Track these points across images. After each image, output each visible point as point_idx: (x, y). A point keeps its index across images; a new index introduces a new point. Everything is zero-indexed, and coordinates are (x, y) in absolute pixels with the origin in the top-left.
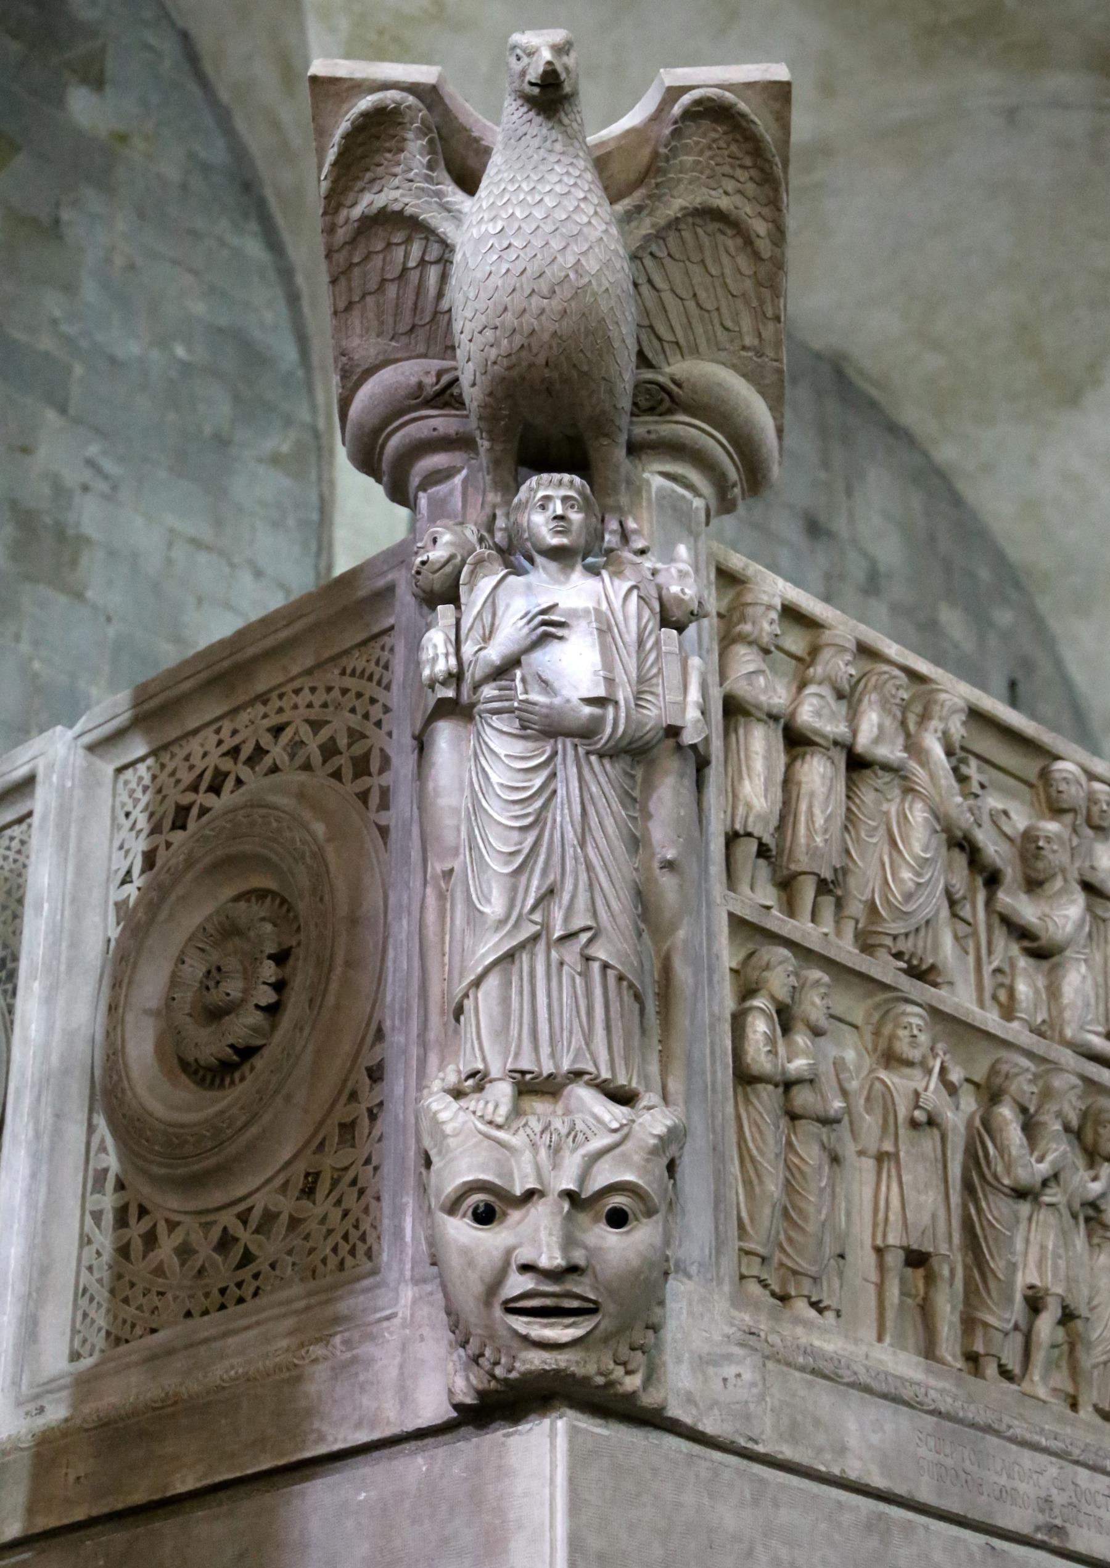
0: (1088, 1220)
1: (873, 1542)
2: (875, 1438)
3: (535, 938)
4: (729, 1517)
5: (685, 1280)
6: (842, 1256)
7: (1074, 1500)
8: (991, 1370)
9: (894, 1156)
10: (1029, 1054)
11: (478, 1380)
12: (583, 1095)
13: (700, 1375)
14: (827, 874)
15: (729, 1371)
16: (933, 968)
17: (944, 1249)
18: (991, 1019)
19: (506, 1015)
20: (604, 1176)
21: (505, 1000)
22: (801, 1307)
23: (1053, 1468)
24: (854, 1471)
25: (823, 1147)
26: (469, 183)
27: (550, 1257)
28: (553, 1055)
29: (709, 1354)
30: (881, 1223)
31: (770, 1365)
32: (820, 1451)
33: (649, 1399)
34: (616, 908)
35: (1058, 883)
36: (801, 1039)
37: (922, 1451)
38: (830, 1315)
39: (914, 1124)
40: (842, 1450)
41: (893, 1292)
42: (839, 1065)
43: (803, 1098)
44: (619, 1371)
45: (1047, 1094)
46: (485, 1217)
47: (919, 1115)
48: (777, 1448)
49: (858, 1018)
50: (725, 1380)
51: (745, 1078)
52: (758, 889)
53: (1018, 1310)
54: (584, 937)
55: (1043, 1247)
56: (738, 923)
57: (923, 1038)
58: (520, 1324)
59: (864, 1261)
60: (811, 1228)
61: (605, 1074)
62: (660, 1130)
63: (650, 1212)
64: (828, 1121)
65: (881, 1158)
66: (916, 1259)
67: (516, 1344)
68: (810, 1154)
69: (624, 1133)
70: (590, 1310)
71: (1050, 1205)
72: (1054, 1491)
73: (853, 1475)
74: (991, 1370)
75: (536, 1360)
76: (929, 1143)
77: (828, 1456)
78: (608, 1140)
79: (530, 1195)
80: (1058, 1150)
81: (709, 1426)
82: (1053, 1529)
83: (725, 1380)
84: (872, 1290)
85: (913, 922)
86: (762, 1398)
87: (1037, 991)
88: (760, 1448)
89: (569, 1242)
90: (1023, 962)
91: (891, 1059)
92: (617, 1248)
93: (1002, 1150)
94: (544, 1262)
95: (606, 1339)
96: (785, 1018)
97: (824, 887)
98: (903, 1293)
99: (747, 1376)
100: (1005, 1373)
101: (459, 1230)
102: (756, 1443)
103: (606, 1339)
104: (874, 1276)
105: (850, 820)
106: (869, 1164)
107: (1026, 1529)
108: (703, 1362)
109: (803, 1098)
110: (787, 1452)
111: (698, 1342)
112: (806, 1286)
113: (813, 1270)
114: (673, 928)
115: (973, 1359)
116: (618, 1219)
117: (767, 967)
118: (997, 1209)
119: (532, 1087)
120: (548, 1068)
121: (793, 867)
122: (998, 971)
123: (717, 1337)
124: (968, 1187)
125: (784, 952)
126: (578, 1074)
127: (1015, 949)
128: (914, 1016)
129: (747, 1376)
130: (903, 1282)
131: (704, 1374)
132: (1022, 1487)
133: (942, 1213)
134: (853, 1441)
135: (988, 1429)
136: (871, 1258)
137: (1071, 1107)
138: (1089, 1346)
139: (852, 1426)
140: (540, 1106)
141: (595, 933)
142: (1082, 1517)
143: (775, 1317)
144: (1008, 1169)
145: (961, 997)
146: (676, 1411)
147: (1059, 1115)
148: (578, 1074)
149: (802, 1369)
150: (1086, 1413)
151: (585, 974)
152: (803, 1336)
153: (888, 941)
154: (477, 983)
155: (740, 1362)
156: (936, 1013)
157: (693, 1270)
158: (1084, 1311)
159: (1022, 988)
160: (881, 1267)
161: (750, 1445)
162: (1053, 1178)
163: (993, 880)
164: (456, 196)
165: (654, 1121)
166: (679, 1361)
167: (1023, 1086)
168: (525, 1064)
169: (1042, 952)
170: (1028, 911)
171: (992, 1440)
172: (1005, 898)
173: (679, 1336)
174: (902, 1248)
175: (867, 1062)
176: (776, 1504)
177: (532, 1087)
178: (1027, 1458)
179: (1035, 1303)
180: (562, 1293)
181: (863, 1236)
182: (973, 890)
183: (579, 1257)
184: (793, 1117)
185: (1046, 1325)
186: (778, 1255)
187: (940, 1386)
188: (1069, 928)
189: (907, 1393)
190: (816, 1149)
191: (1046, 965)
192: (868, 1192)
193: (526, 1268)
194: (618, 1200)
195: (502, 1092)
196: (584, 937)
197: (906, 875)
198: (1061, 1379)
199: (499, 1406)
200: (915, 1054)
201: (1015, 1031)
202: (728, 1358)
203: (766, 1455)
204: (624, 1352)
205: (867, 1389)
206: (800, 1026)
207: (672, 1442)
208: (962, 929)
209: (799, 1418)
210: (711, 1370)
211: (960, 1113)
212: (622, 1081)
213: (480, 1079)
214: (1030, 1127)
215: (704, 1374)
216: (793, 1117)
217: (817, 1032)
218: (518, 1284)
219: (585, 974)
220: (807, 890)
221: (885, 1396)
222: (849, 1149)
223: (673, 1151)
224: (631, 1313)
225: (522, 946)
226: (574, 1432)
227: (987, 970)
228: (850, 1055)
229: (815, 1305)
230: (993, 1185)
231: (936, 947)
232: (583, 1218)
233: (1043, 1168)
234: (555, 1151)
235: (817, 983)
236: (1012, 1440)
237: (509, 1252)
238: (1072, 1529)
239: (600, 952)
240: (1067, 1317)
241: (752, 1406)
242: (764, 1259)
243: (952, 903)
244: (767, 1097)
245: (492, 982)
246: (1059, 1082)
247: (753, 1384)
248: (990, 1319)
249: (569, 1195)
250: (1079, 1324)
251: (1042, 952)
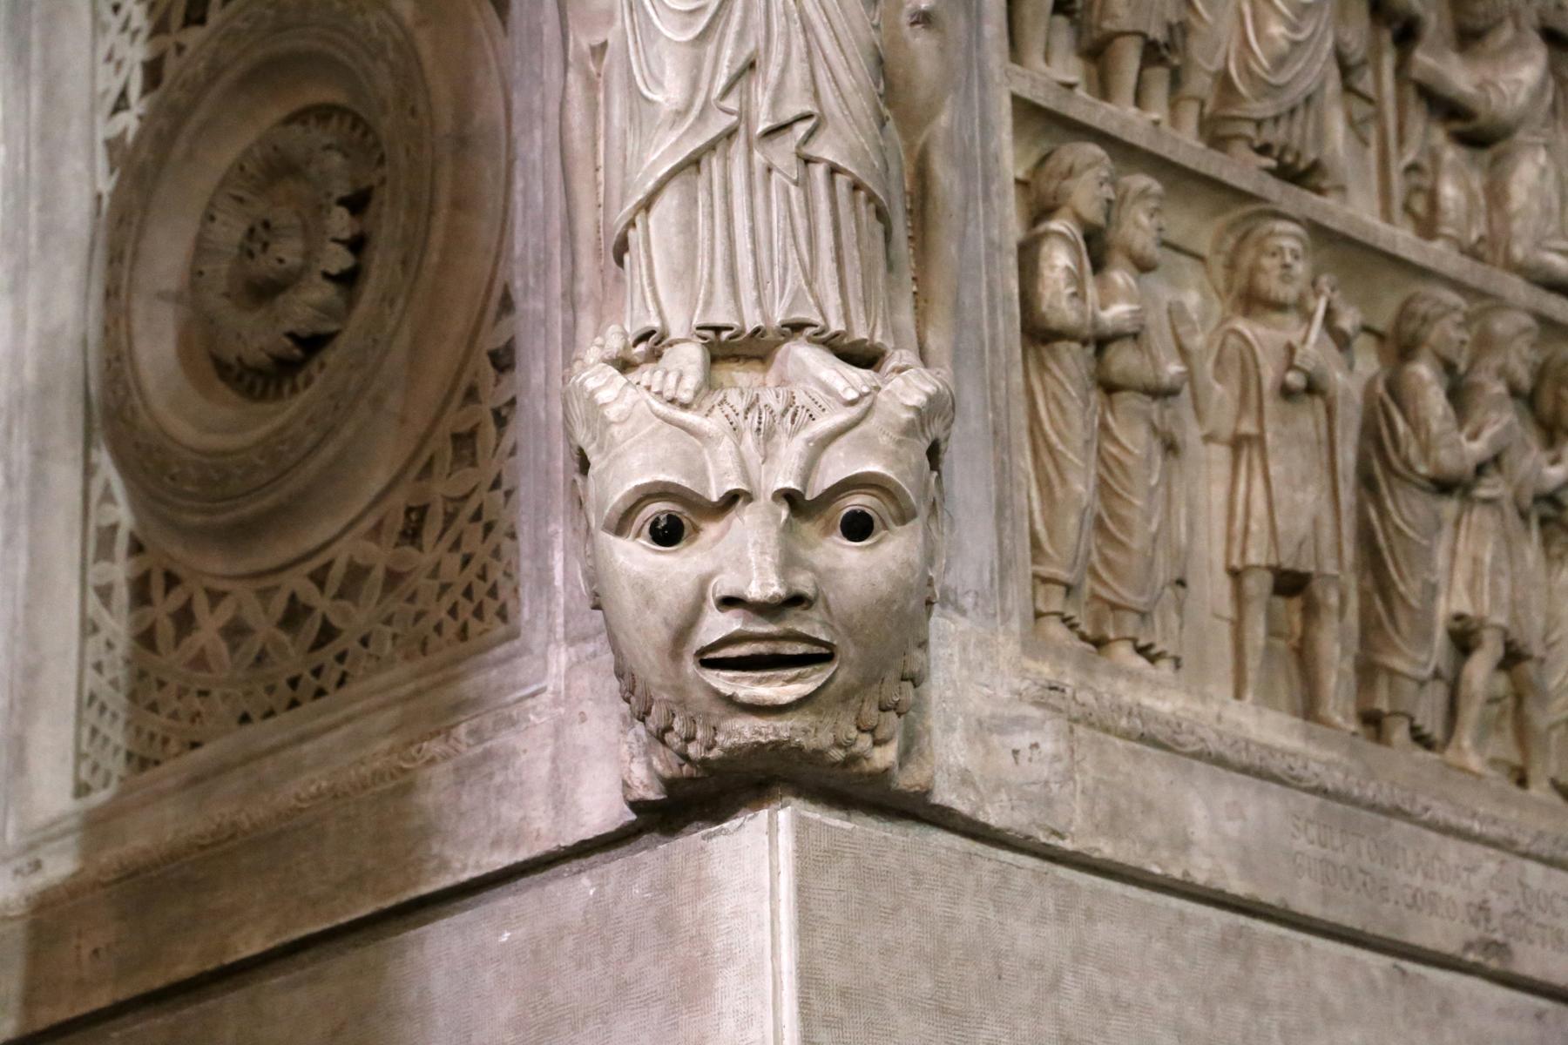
0: (1544, 521)
1: (1231, 966)
2: (1232, 828)
3: (730, 134)
4: (1025, 936)
5: (956, 616)
6: (1181, 583)
7: (1522, 907)
8: (1400, 734)
9: (1260, 440)
10: (1457, 285)
11: (666, 763)
12: (804, 356)
13: (979, 747)
14: (1157, 33)
15: (1022, 740)
16: (1315, 167)
17: (1330, 568)
18: (1402, 239)
19: (691, 247)
20: (837, 467)
21: (689, 228)
22: (1123, 652)
23: (1490, 863)
24: (1201, 871)
25: (1154, 430)
27: (763, 585)
28: (759, 302)
29: (993, 716)
30: (1236, 536)
31: (1080, 730)
32: (1152, 845)
33: (908, 780)
34: (847, 88)
35: (1507, 33)
36: (1120, 276)
37: (1301, 844)
38: (1165, 666)
39: (1286, 392)
40: (1184, 844)
41: (1257, 631)
42: (1176, 313)
43: (1123, 360)
44: (865, 741)
45: (1485, 343)
46: (668, 534)
47: (1295, 379)
48: (1092, 844)
49: (1204, 245)
50: (1015, 752)
51: (1039, 334)
52: (1057, 59)
54: (801, 129)
55: (1476, 561)
56: (1026, 110)
57: (1300, 268)
58: (722, 681)
59: (1213, 589)
60: (1136, 544)
61: (836, 325)
62: (917, 399)
63: (904, 517)
64: (1161, 393)
65: (1238, 443)
66: (1290, 583)
67: (717, 710)
68: (1134, 439)
69: (865, 407)
70: (822, 656)
71: (1488, 501)
72: (1492, 895)
73: (1200, 878)
74: (1400, 734)
75: (746, 730)
76: (1308, 418)
77: (1165, 854)
78: (843, 416)
79: (732, 499)
80: (1499, 421)
81: (994, 816)
82: (1489, 946)
83: (1015, 752)
84: (1225, 630)
85: (1287, 99)
86: (1068, 777)
87: (1471, 196)
88: (1068, 845)
89: (789, 563)
90: (1451, 153)
91: (1253, 301)
92: (857, 569)
93: (1416, 425)
94: (754, 592)
95: (846, 696)
96: (1097, 247)
97: (1153, 53)
98: (1273, 632)
99: (1048, 747)
100: (1420, 739)
101: (633, 556)
102: (1061, 836)
103: (846, 696)
104: (1228, 610)
106: (1220, 453)
107: (1451, 947)
108: (983, 729)
109: (1123, 360)
110: (1106, 849)
111: (977, 701)
112: (1130, 623)
113: (1139, 601)
114: (932, 110)
115: (1373, 722)
116: (858, 528)
117: (1070, 173)
118: (1409, 510)
119: (731, 349)
120: (752, 320)
121: (1108, 25)
122: (1413, 168)
123: (1003, 694)
124: (1367, 481)
125: (1094, 150)
126: (796, 328)
127: (1439, 135)
128: (1287, 237)
129: (1048, 747)
130: (1271, 617)
131: (985, 743)
132: (1445, 890)
133: (1327, 519)
134: (1200, 832)
135: (1396, 812)
136: (1224, 585)
137: (1520, 360)
138: (1544, 698)
139: (1198, 812)
140: (741, 377)
141: (816, 122)
142: (1533, 929)
143: (1085, 666)
144: (1426, 450)
145: (1358, 209)
146: (946, 795)
147: (1502, 373)
148: (797, 328)
149: (1126, 735)
150: (1539, 790)
151: (803, 183)
152: (1125, 692)
153: (1249, 130)
154: (647, 205)
155: (1038, 727)
156: (1320, 234)
157: (968, 602)
158: (1537, 650)
159: (1449, 191)
160: (1239, 597)
161: (1053, 841)
163: (1407, 34)
165: (907, 388)
166: (949, 728)
167: (1448, 333)
168: (720, 319)
169: (1479, 135)
170: (1460, 77)
171: (1401, 827)
172: (1423, 59)
173: (949, 693)
174: (1269, 568)
175: (1217, 308)
176: (1090, 916)
177: (731, 349)
178: (1453, 851)
179: (1464, 640)
180: (780, 635)
181: (1212, 554)
182: (1376, 51)
183: (804, 583)
184: (1110, 388)
185: (1480, 670)
186: (1089, 583)
187: (1323, 758)
188: (1522, 98)
189: (1277, 765)
190: (1142, 432)
191: (1486, 156)
192: (1219, 493)
193: (728, 602)
194: (857, 501)
195: (688, 358)
196: (801, 129)
197: (1276, 29)
198: (1503, 746)
199: (696, 797)
200: (1288, 293)
201: (1438, 254)
202: (1020, 722)
203: (1076, 853)
204: (871, 713)
205: (1220, 761)
206: (1118, 258)
207: (942, 840)
208: (1360, 109)
209: (1123, 803)
210: (995, 740)
211: (1353, 377)
212: (860, 333)
213: (654, 342)
214: (1459, 394)
215: (985, 743)
216: (1110, 388)
217: (1143, 266)
218: (718, 625)
219: (803, 183)
220: (1129, 59)
221: (1245, 770)
222: (1191, 434)
223: (936, 429)
224: (882, 659)
225: (711, 147)
226: (802, 827)
227: (1397, 167)
228: (1192, 299)
229: (1142, 651)
230: (1402, 475)
231: (1321, 135)
232: (809, 529)
233: (1478, 449)
234: (767, 435)
235: (1144, 194)
236: (1432, 826)
237: (703, 583)
238: (1517, 947)
239: (826, 150)
240: (1512, 658)
241: (1055, 787)
242: (1069, 589)
243: (1346, 69)
244: (1071, 360)
245: (669, 202)
246: (1502, 325)
247: (1056, 758)
248: (1398, 664)
249: (790, 498)
250: (1529, 668)
251: (1479, 135)
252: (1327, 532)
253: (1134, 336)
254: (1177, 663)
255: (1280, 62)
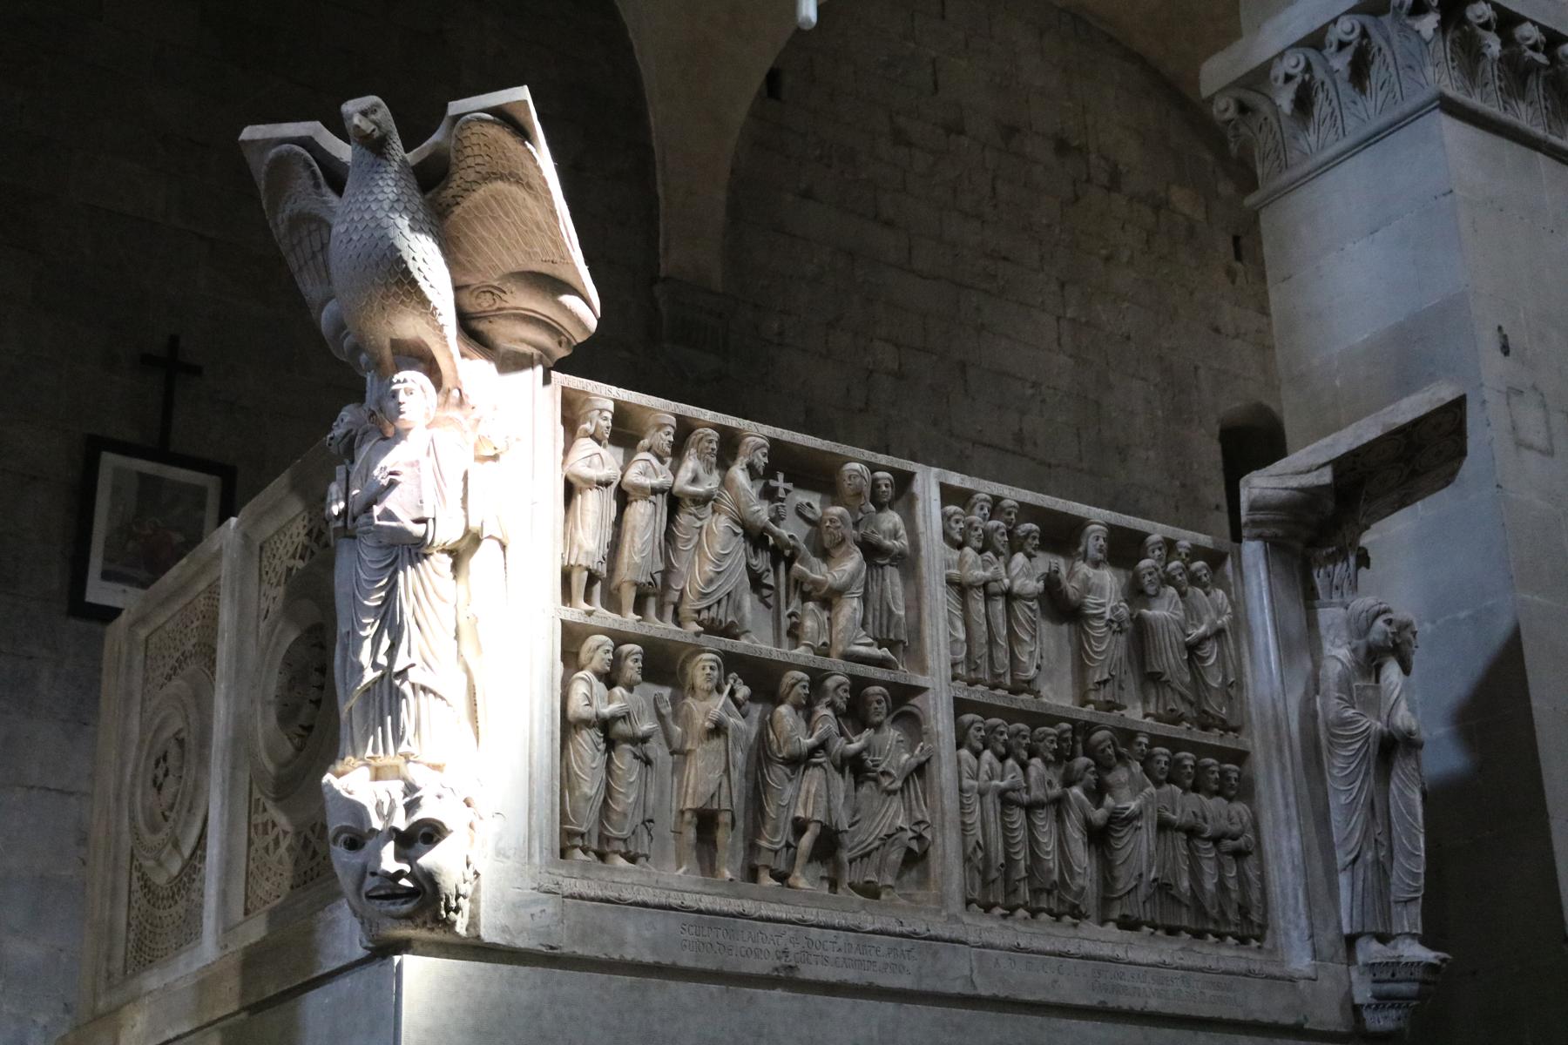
2: (647, 934)
17: (725, 805)
26: (338, 186)
38: (642, 860)
40: (621, 943)
53: (785, 835)
71: (820, 764)
72: (790, 946)
105: (670, 536)
133: (725, 784)
142: (812, 958)
147: (831, 705)
150: (842, 892)
162: (823, 746)
164: (331, 197)
190: (628, 757)
233: (811, 741)
237: (364, 867)
238: (802, 967)
252: (725, 790)
253: (625, 717)
254: (647, 858)
255: (710, 582)
